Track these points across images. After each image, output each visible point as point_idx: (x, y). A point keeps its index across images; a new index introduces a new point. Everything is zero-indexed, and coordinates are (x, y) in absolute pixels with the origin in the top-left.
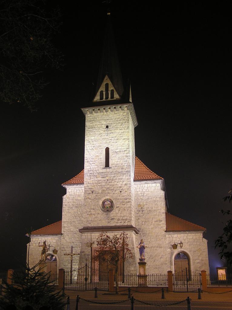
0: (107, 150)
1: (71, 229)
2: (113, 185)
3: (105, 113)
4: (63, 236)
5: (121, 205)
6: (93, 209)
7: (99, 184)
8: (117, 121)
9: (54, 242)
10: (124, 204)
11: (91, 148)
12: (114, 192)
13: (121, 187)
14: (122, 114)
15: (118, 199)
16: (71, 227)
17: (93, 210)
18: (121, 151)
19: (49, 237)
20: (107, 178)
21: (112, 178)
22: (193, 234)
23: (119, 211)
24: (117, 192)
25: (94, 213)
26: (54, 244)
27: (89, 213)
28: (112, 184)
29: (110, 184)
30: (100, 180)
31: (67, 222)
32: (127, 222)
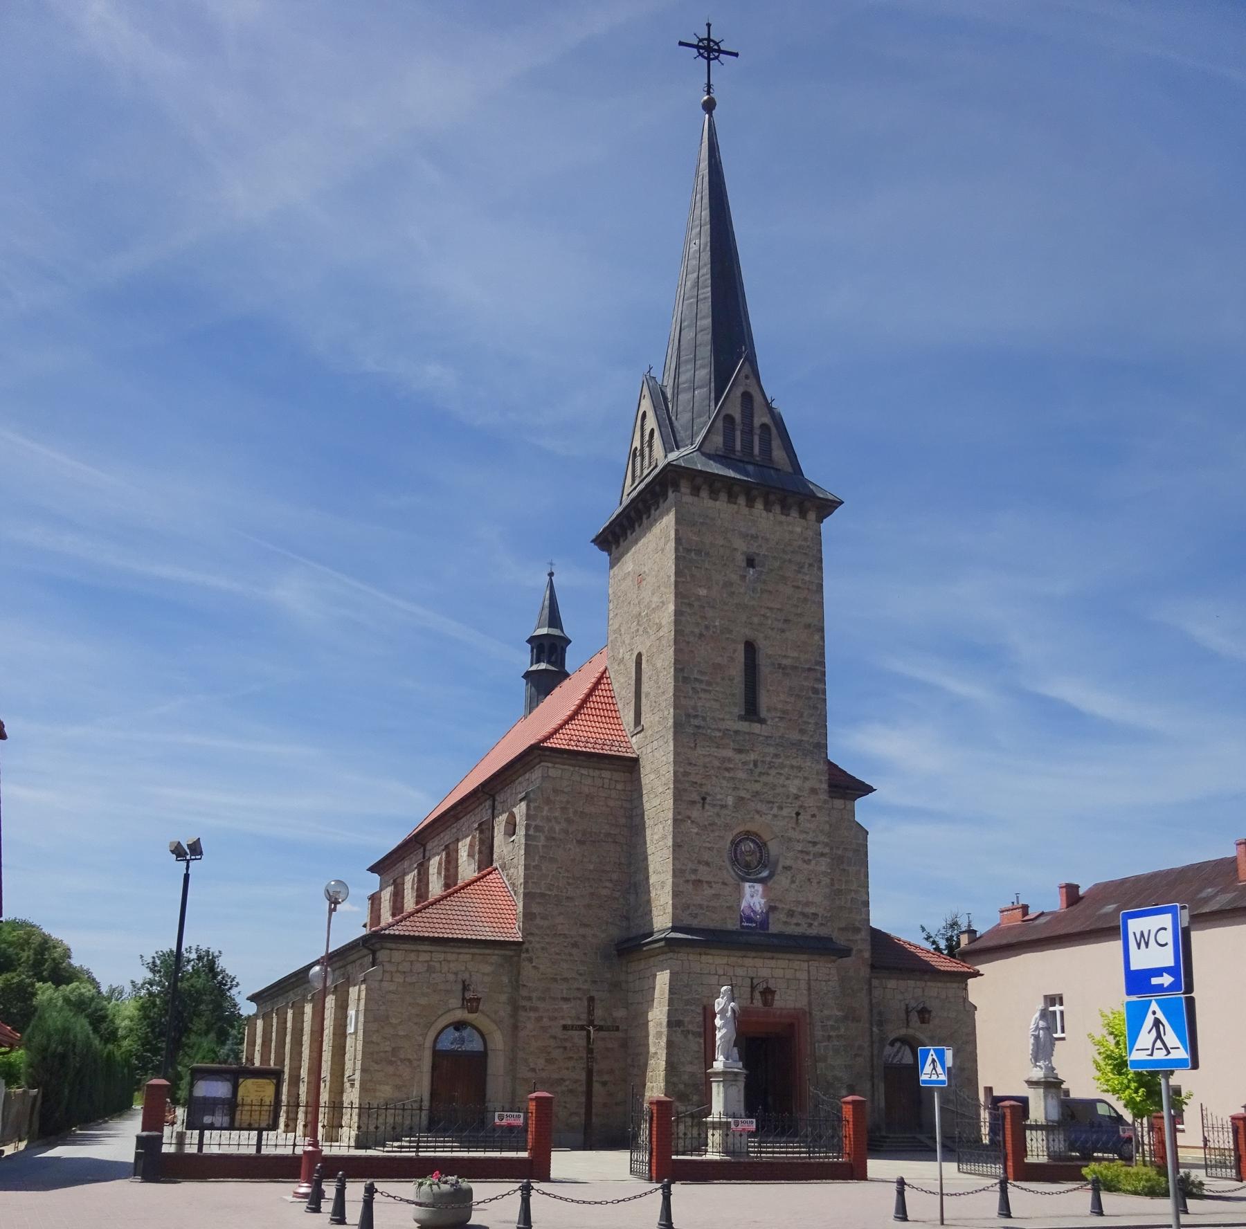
0: (750, 648)
1: (560, 927)
2: (774, 787)
3: (745, 510)
4: (527, 951)
5: (800, 862)
6: (707, 864)
7: (727, 774)
8: (784, 552)
9: (484, 974)
10: (807, 858)
11: (697, 631)
12: (775, 811)
13: (797, 797)
14: (798, 530)
15: (790, 839)
16: (560, 919)
17: (705, 868)
18: (796, 668)
19: (466, 950)
20: (753, 756)
21: (768, 759)
22: (939, 985)
23: (793, 882)
24: (785, 812)
25: (709, 878)
26: (487, 979)
27: (693, 877)
28: (770, 779)
29: (764, 779)
30: (730, 760)
31: (542, 895)
32: (816, 924)
